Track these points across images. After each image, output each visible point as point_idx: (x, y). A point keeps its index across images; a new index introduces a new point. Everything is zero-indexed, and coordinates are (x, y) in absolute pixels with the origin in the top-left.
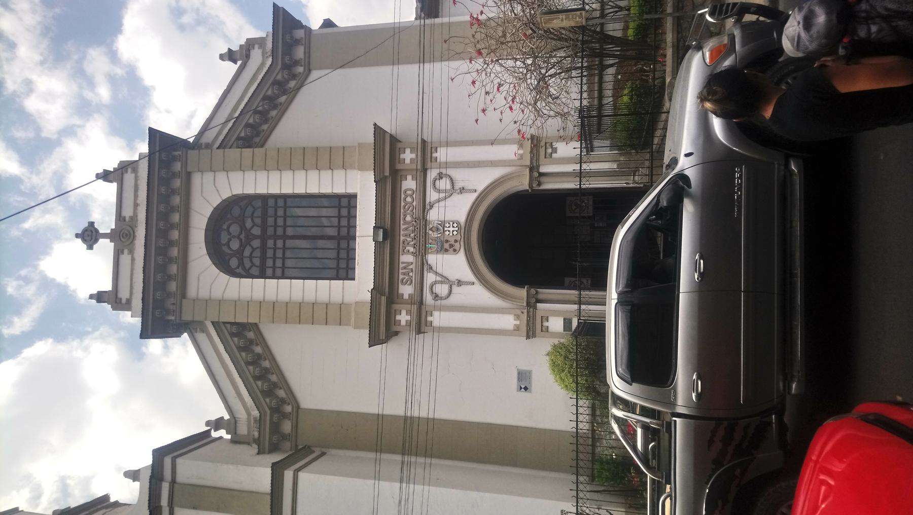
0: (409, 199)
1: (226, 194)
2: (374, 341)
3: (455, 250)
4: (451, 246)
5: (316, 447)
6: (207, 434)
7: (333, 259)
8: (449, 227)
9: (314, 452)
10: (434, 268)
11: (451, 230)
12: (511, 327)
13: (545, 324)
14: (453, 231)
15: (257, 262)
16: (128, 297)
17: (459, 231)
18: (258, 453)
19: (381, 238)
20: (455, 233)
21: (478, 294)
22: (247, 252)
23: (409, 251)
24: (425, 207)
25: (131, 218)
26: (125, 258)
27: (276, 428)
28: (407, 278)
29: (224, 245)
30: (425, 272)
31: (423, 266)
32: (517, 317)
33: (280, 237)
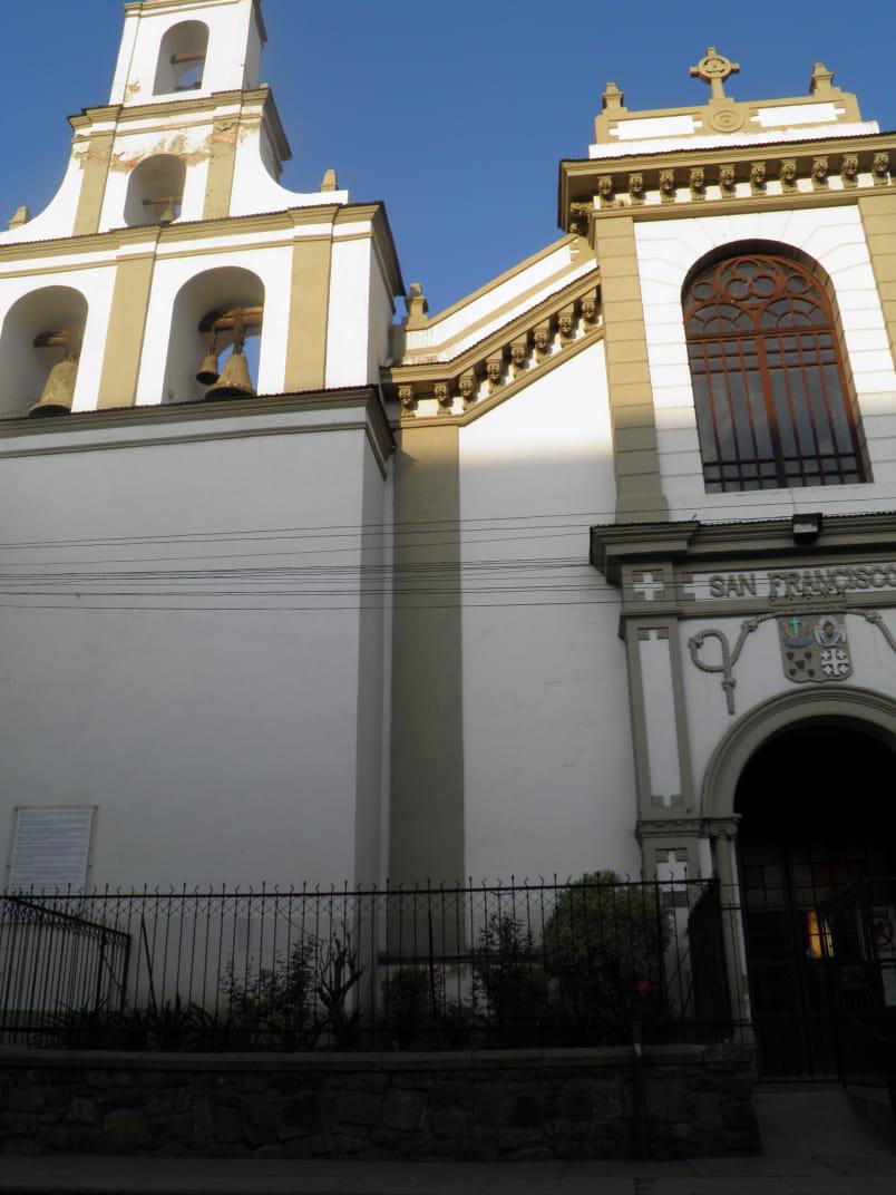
0: (879, 578)
3: (792, 672)
4: (800, 665)
5: (394, 462)
7: (737, 454)
8: (838, 658)
9: (386, 459)
10: (751, 636)
11: (832, 662)
12: (656, 790)
13: (672, 856)
14: (831, 666)
15: (713, 328)
16: (621, 138)
17: (832, 677)
18: (381, 368)
19: (799, 529)
21: (711, 723)
23: (777, 585)
24: (868, 608)
25: (758, 124)
27: (423, 391)
28: (726, 588)
29: (733, 274)
30: (740, 621)
31: (754, 614)
32: (677, 801)
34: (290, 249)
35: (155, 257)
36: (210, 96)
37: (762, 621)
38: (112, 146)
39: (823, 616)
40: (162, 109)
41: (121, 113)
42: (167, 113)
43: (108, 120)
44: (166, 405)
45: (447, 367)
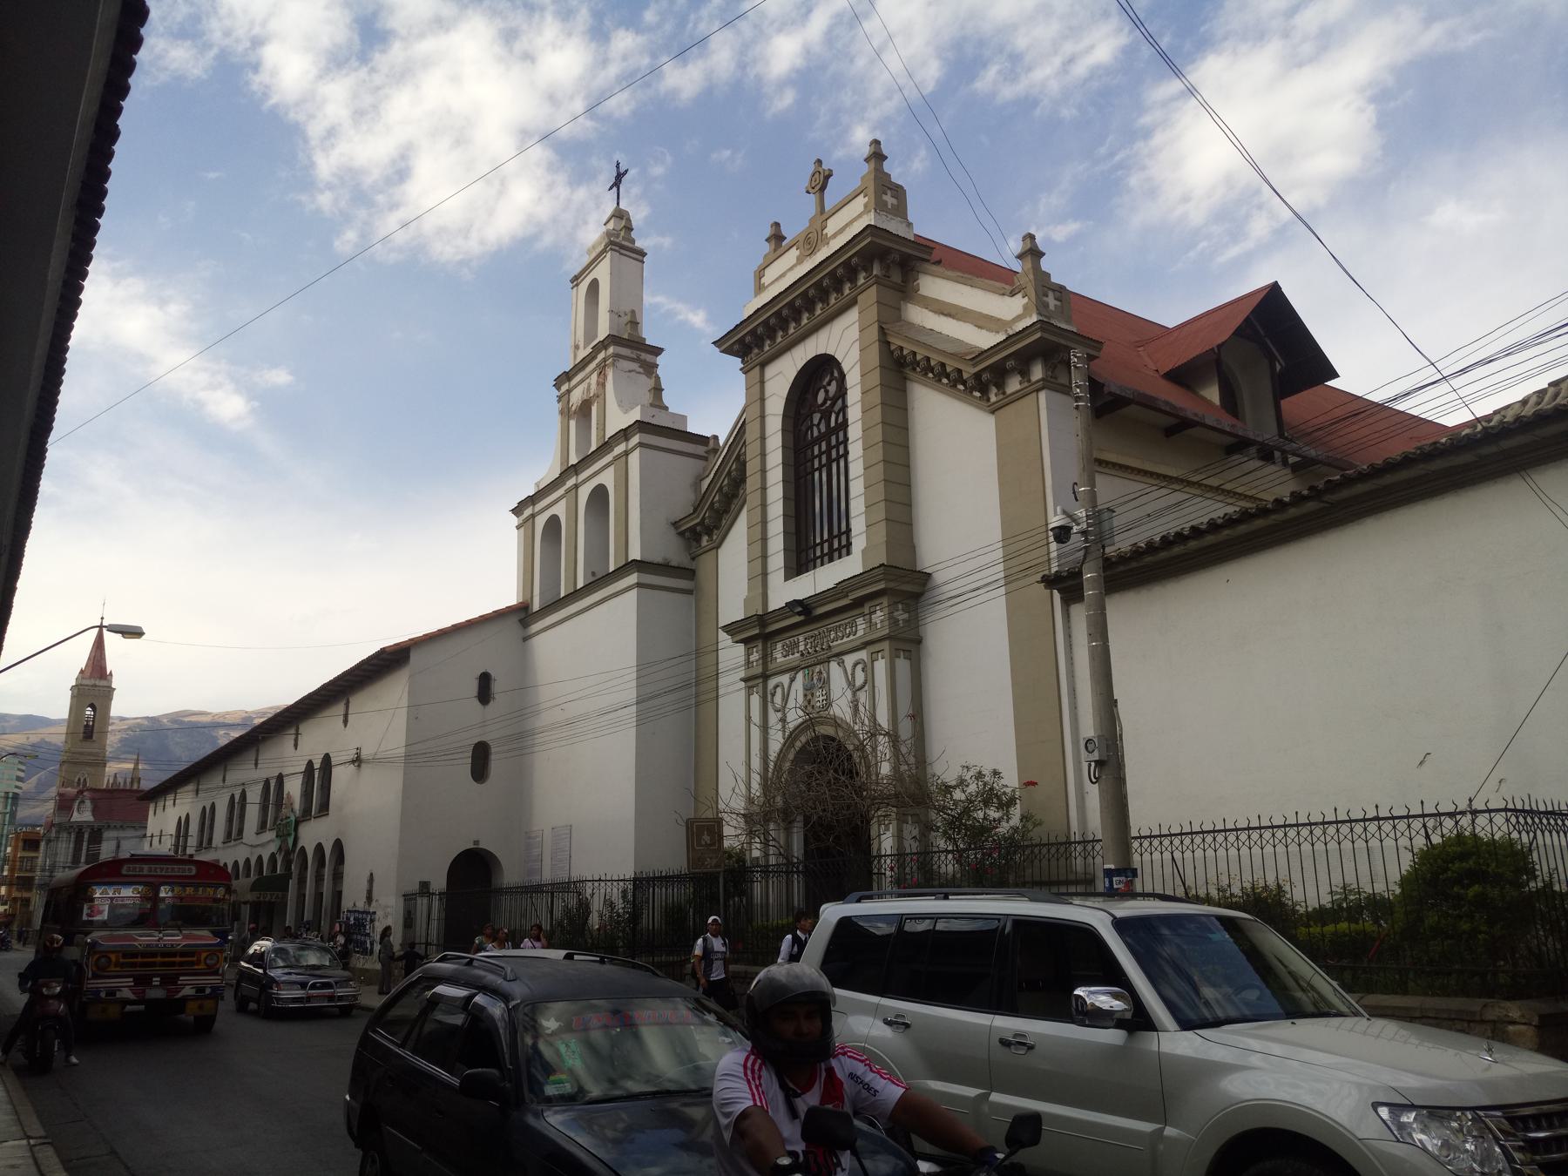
1: (845, 367)
4: (809, 702)
9: (693, 580)
11: (819, 697)
20: (818, 704)
21: (775, 746)
26: (794, 253)
31: (794, 669)
34: (612, 469)
35: (576, 486)
37: (796, 674)
38: (569, 402)
39: (818, 666)
42: (583, 368)
43: (564, 383)
44: (587, 585)
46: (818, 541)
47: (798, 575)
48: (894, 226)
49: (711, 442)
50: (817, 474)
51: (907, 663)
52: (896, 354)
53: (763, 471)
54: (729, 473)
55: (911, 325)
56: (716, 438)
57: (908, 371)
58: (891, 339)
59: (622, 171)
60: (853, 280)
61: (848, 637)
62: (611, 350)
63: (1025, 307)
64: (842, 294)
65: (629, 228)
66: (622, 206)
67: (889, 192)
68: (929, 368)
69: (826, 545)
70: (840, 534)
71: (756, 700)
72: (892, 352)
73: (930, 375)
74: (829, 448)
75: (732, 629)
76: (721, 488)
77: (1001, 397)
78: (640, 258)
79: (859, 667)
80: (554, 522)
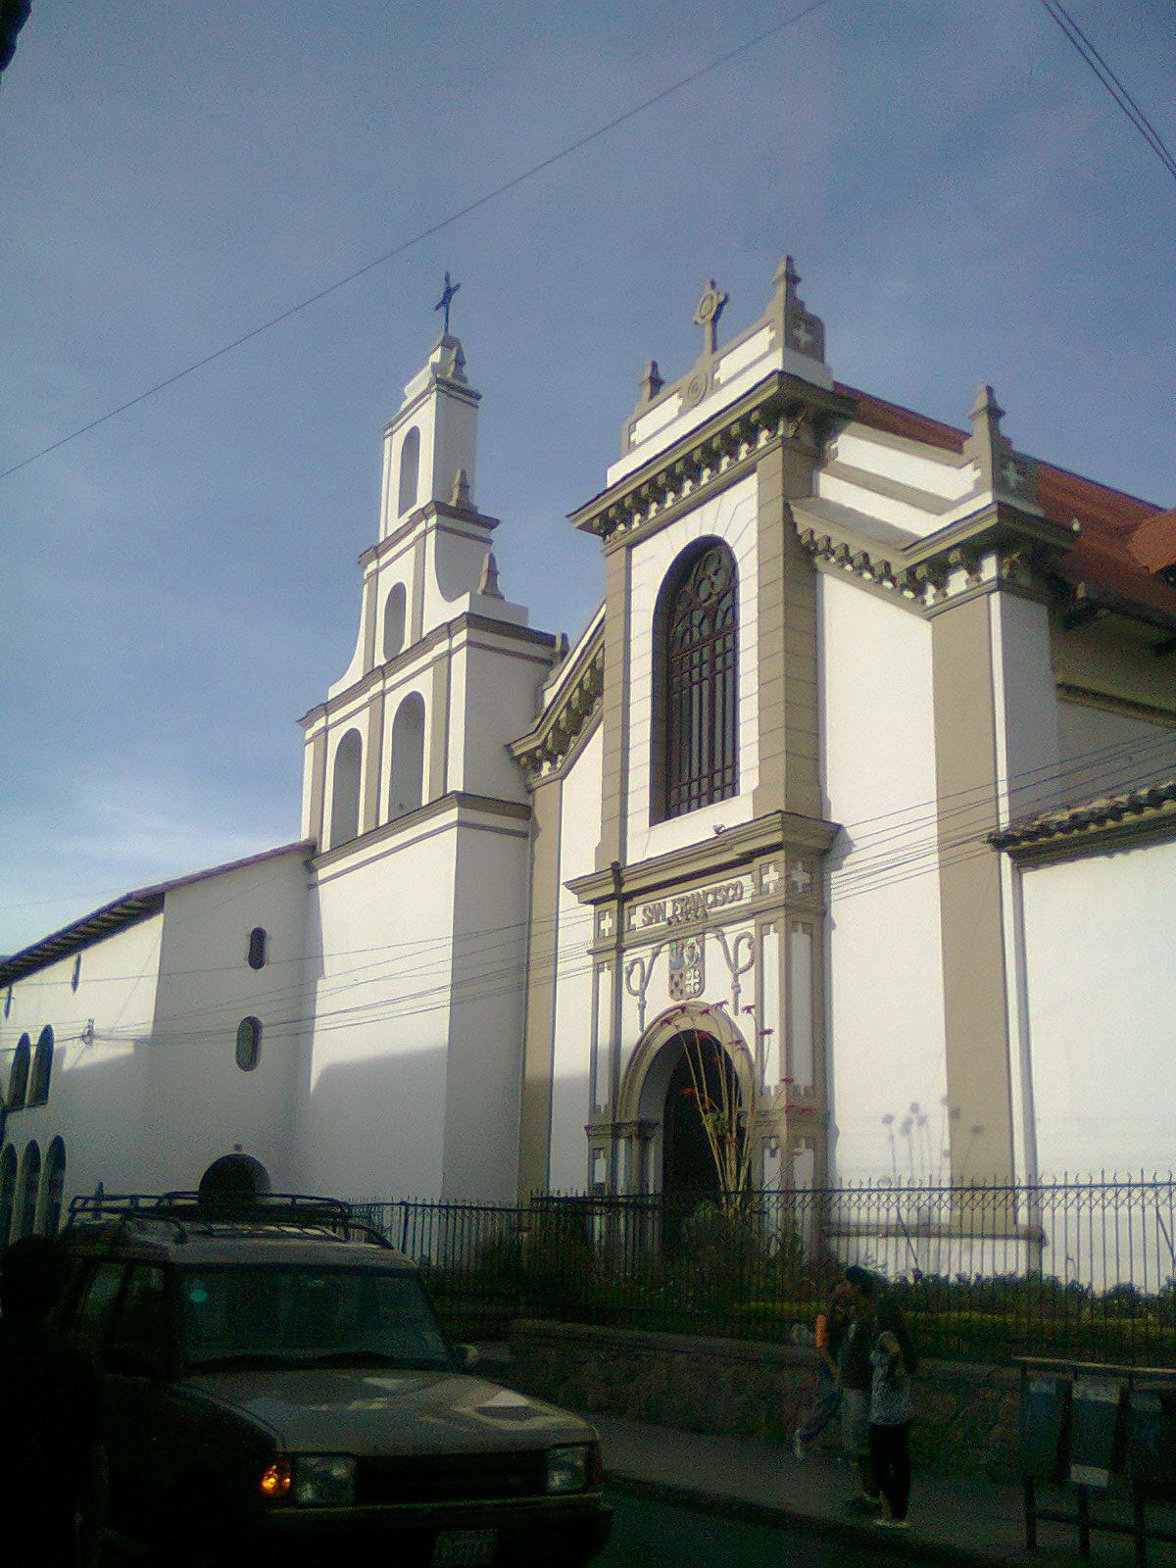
0: (731, 892)
1: (738, 554)
2: (576, 886)
3: (672, 992)
4: (677, 985)
6: (547, 640)
8: (695, 978)
11: (691, 981)
22: (697, 616)
24: (717, 927)
31: (656, 939)
33: (713, 665)
35: (383, 694)
36: (408, 520)
37: (662, 945)
40: (394, 538)
41: (377, 551)
45: (535, 735)
46: (695, 775)
47: (668, 817)
48: (808, 371)
49: (558, 642)
50: (696, 689)
51: (806, 939)
52: (805, 540)
53: (626, 683)
54: (580, 685)
55: (827, 502)
56: (564, 637)
57: (818, 560)
58: (796, 519)
59: (452, 286)
60: (752, 441)
61: (730, 902)
62: (433, 520)
63: (978, 483)
64: (737, 459)
65: (460, 362)
66: (452, 332)
67: (803, 326)
68: (846, 558)
69: (705, 782)
70: (723, 771)
71: (606, 977)
72: (800, 537)
73: (849, 567)
74: (714, 655)
75: (576, 886)
76: (569, 703)
77: (941, 599)
78: (473, 400)
79: (745, 942)
80: (353, 738)
